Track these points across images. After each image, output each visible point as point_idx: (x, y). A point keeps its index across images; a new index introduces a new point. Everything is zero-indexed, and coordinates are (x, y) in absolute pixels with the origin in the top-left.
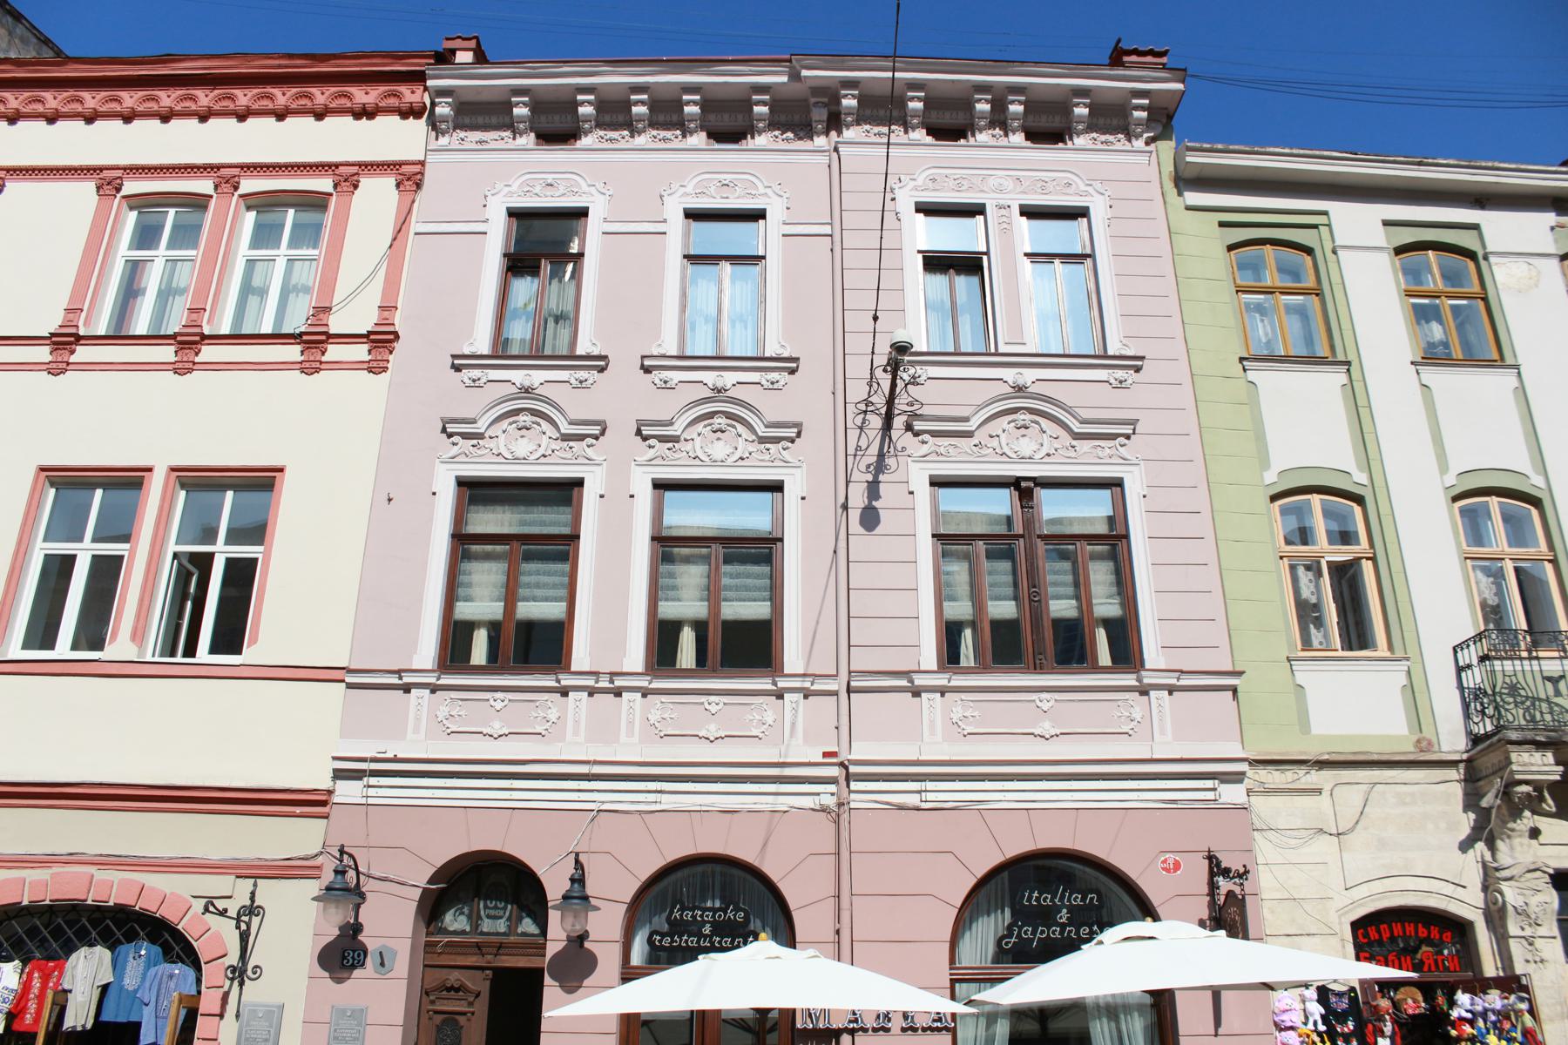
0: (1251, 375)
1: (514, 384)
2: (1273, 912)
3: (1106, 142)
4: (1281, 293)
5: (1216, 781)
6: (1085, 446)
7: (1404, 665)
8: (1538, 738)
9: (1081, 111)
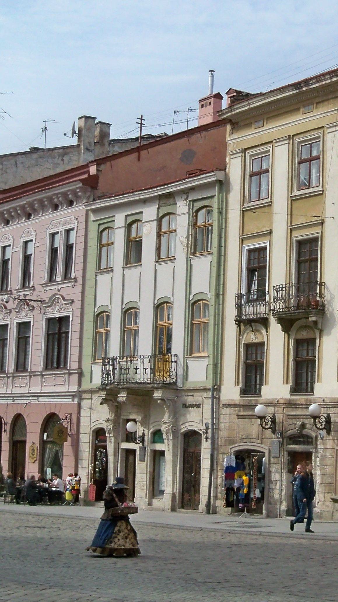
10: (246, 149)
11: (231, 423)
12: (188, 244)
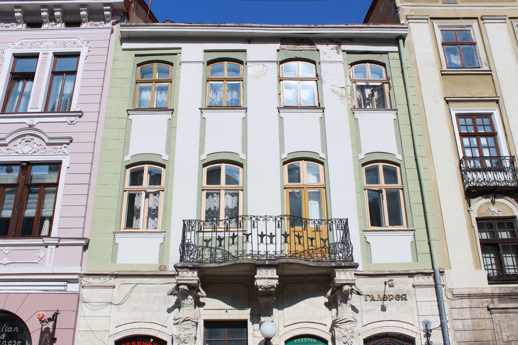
0: (131, 117)
1: (26, 124)
2: (82, 336)
3: (95, 25)
4: (155, 82)
5: (66, 282)
6: (50, 148)
7: (164, 235)
8: (189, 266)
9: (83, 13)
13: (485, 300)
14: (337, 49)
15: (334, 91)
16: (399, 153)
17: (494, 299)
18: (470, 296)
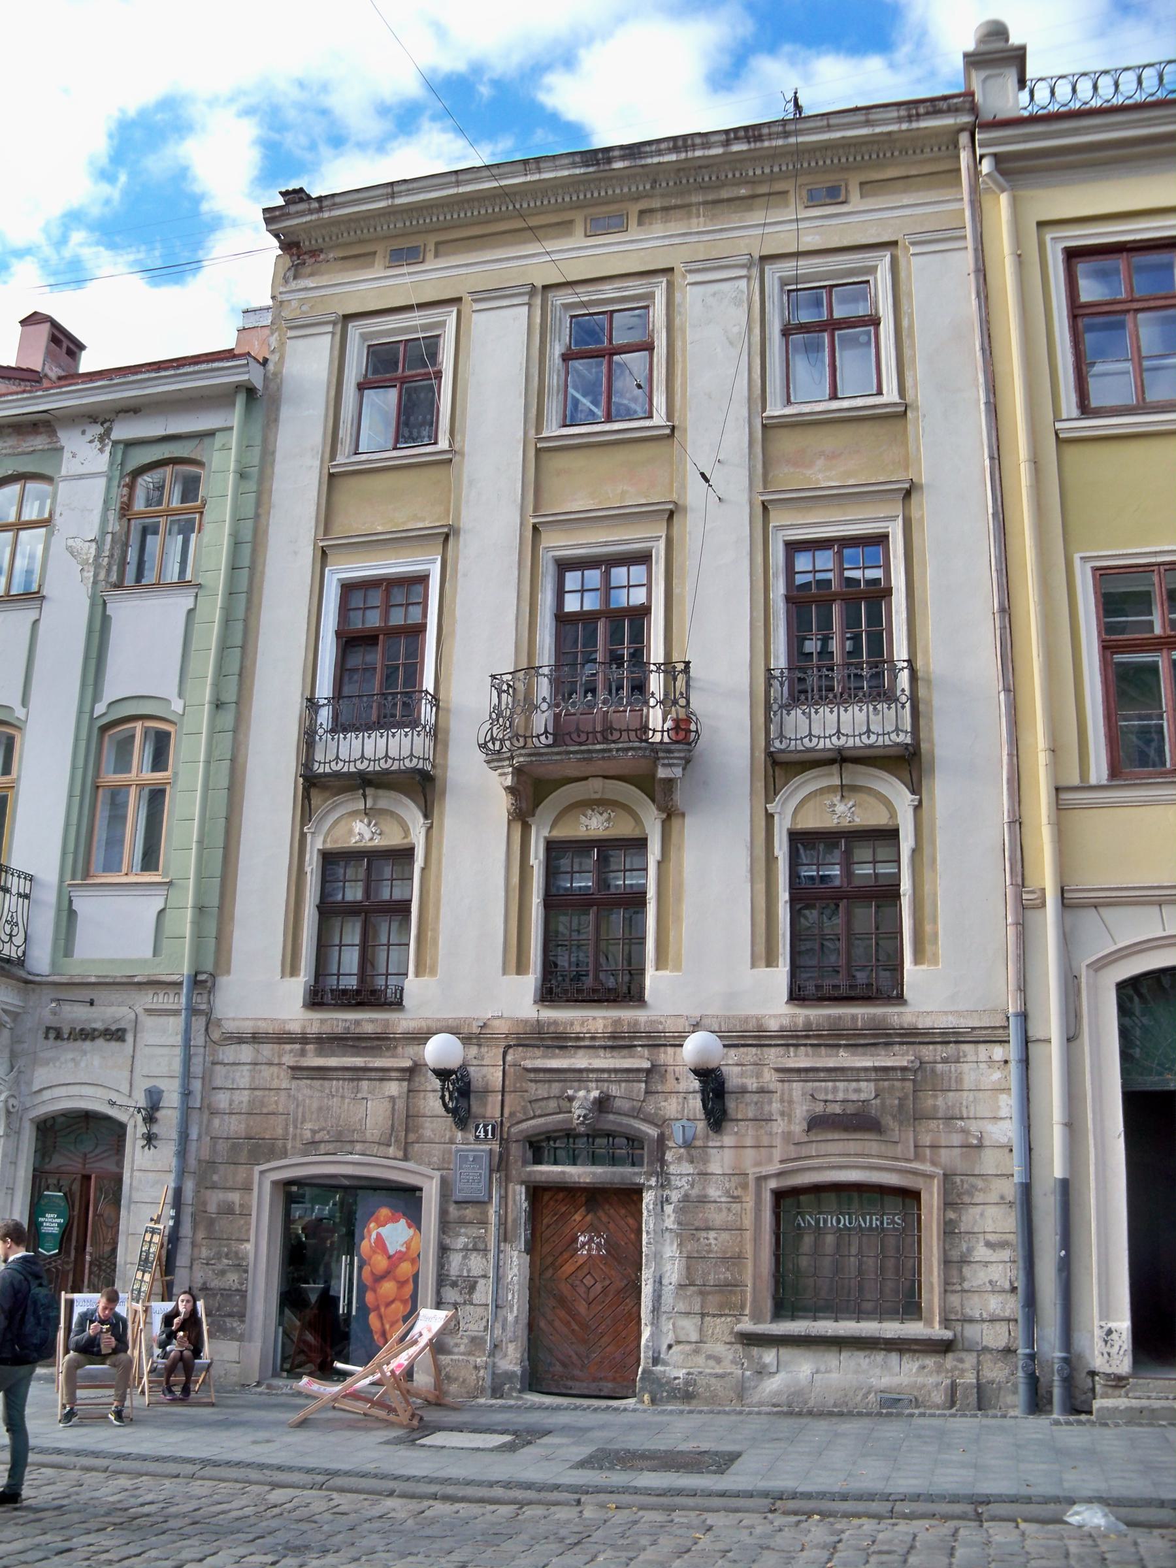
10: (348, 318)
11: (258, 1093)
12: (97, 557)
13: (288, 1047)
14: (101, 439)
15: (72, 553)
16: (180, 695)
17: (310, 1047)
18: (256, 1038)
